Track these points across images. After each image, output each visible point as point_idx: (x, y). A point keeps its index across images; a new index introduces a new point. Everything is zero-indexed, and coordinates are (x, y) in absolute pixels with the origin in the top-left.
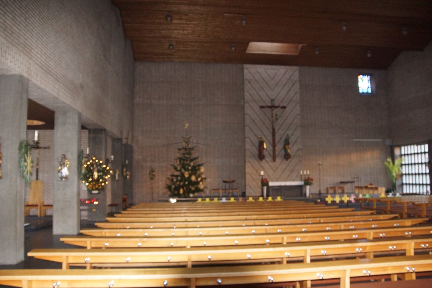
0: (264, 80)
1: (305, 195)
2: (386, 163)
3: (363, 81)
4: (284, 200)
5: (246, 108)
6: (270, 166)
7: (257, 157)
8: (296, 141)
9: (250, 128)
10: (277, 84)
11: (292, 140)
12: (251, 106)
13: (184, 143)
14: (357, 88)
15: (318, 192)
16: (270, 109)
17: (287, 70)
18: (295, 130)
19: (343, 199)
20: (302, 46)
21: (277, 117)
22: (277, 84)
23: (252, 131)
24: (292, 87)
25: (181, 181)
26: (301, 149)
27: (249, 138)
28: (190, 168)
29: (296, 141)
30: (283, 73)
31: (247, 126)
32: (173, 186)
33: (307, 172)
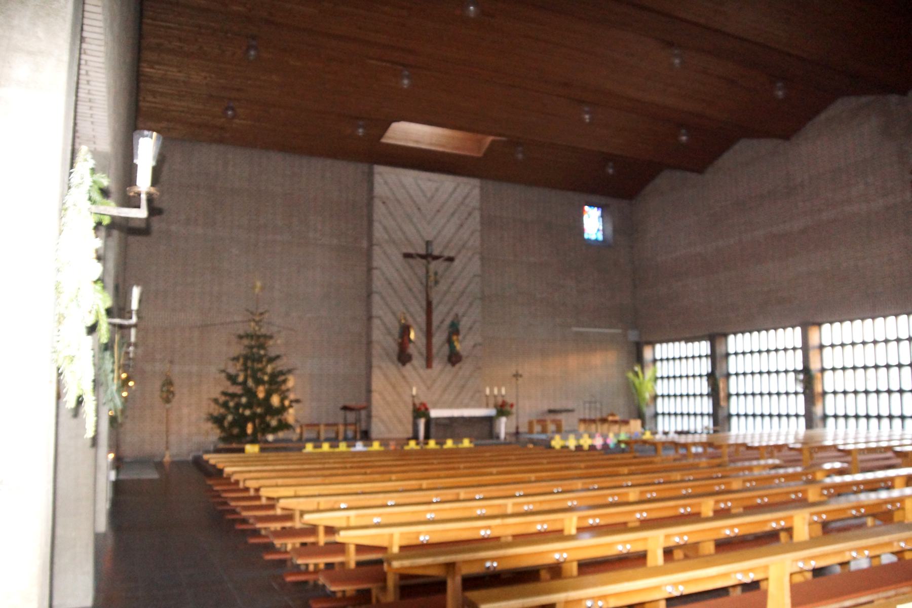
0: (414, 202)
1: (498, 437)
2: (630, 375)
3: (589, 217)
4: (476, 445)
6: (421, 377)
7: (395, 358)
9: (383, 298)
10: (438, 211)
11: (464, 324)
12: (385, 253)
13: (253, 324)
14: (582, 231)
16: (424, 261)
17: (458, 185)
18: (471, 304)
19: (582, 442)
20: (493, 142)
22: (438, 211)
24: (466, 219)
25: (246, 406)
27: (379, 317)
28: (266, 378)
29: (471, 328)
30: (450, 189)
32: (230, 418)
33: (499, 390)
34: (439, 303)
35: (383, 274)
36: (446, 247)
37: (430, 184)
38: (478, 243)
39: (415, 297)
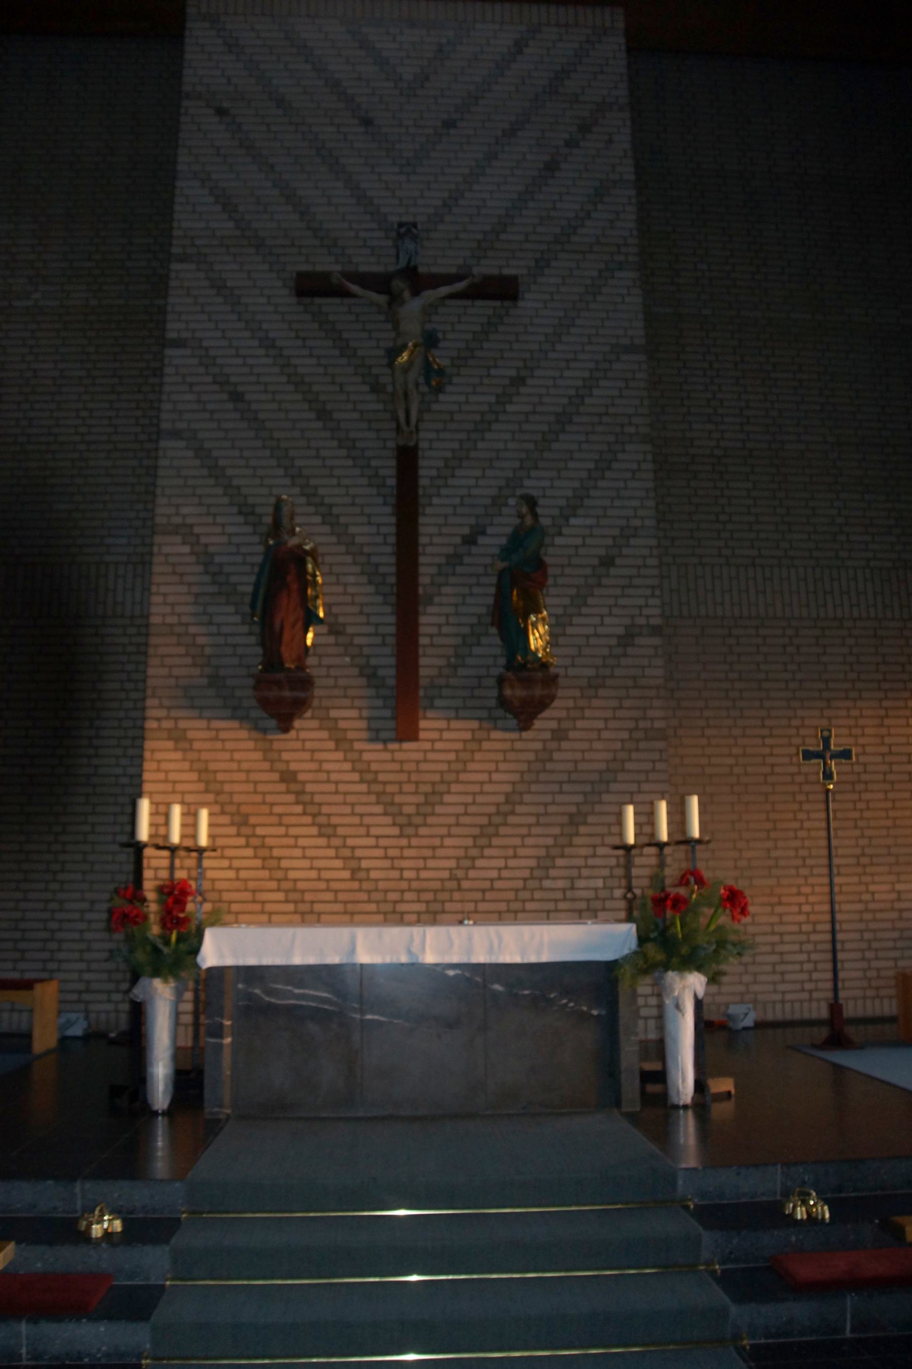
6: (368, 775)
8: (607, 562)
10: (449, 124)
21: (440, 358)
22: (449, 124)
24: (571, 144)
26: (656, 631)
29: (607, 562)
31: (176, 434)
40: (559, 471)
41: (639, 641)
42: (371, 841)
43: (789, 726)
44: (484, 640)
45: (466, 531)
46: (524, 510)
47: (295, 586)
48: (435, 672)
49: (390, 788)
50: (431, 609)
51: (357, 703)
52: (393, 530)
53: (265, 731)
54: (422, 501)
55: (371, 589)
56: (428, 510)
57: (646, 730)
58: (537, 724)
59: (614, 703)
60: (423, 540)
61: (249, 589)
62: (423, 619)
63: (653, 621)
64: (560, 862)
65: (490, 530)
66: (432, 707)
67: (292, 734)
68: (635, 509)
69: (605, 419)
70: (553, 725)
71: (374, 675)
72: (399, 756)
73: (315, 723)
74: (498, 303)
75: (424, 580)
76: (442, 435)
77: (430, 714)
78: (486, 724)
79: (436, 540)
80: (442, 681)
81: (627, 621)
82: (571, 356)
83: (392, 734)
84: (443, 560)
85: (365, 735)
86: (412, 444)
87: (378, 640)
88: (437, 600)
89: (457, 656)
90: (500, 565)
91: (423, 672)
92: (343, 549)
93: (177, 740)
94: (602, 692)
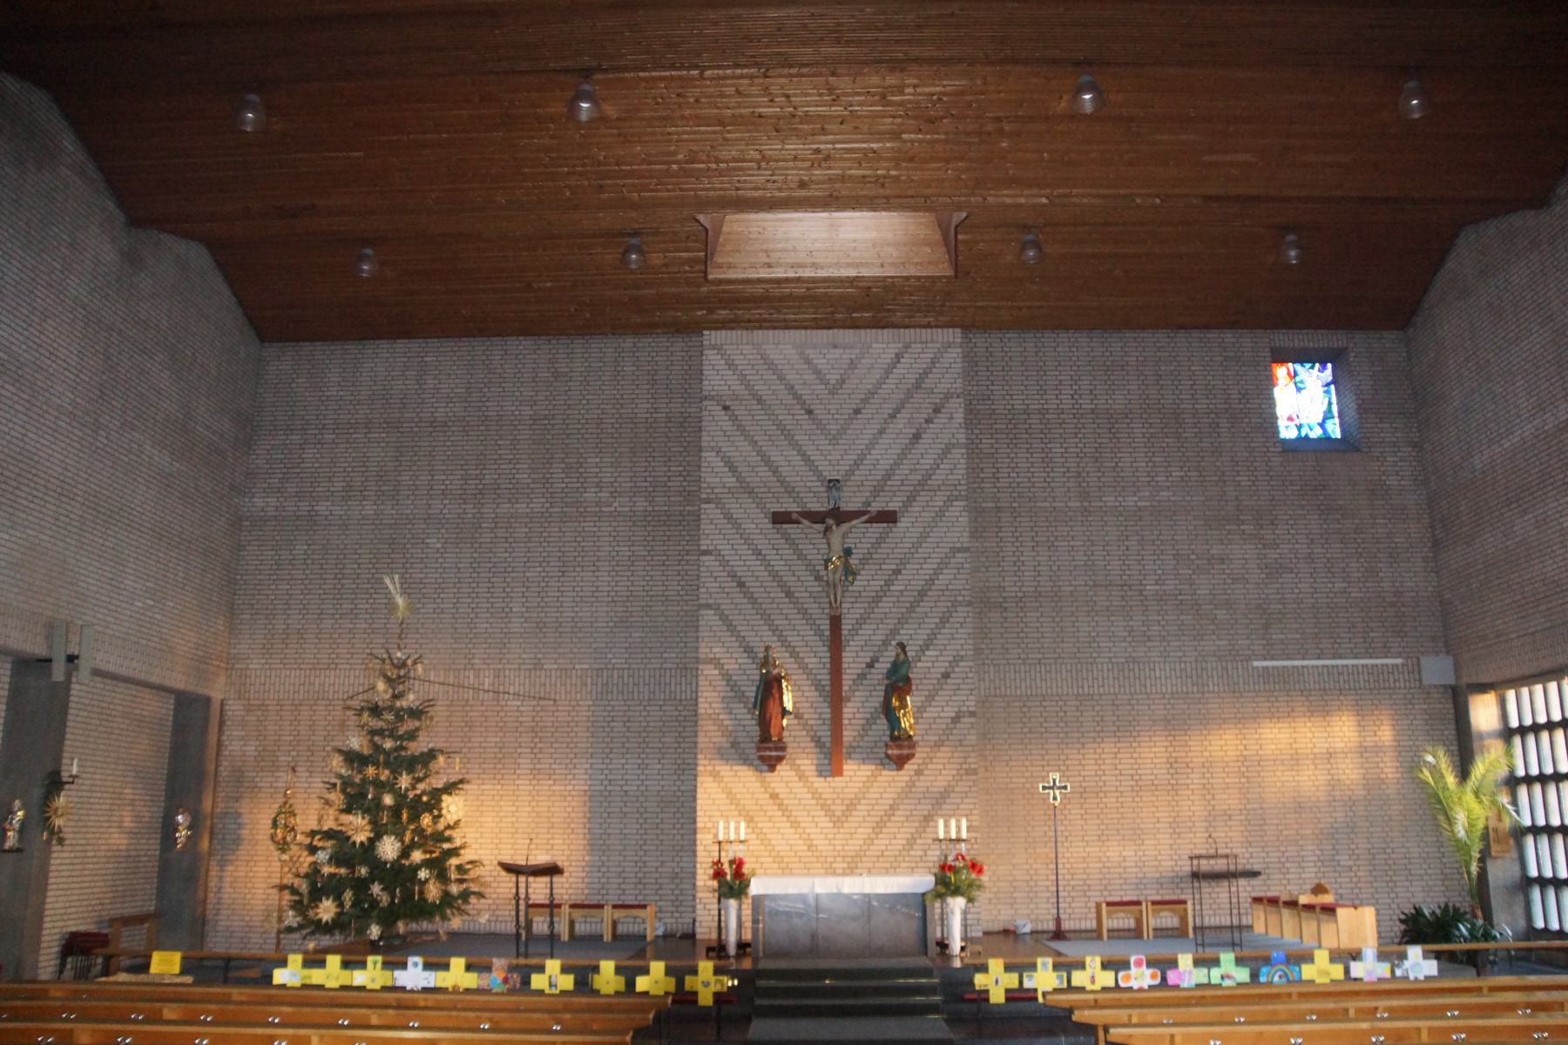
0: (797, 397)
3: (1299, 390)
5: (706, 526)
6: (816, 795)
7: (753, 753)
8: (946, 676)
9: (724, 618)
11: (924, 670)
12: (729, 517)
14: (1268, 421)
15: (1051, 926)
16: (820, 527)
17: (907, 346)
18: (944, 620)
21: (853, 561)
22: (857, 411)
23: (732, 629)
24: (929, 421)
26: (973, 714)
27: (716, 662)
29: (946, 676)
30: (888, 357)
31: (708, 606)
34: (862, 621)
35: (724, 563)
36: (877, 491)
37: (834, 354)
38: (960, 472)
39: (804, 612)
40: (920, 624)
41: (963, 720)
42: (818, 830)
43: (1059, 759)
44: (878, 721)
45: (868, 660)
46: (899, 651)
47: (777, 696)
48: (852, 739)
49: (828, 802)
50: (849, 704)
51: (810, 756)
52: (828, 660)
53: (761, 771)
54: (843, 643)
55: (817, 694)
56: (847, 649)
57: (966, 770)
58: (906, 766)
59: (949, 755)
60: (845, 666)
61: (753, 694)
62: (845, 710)
63: (971, 709)
64: (919, 841)
65: (881, 660)
66: (851, 758)
67: (776, 773)
68: (962, 645)
69: (946, 593)
70: (916, 767)
71: (819, 741)
72: (832, 784)
73: (788, 767)
74: (885, 525)
75: (845, 688)
76: (855, 605)
77: (849, 762)
78: (879, 767)
79: (851, 665)
80: (856, 744)
81: (957, 709)
82: (927, 555)
83: (828, 773)
84: (855, 677)
85: (815, 773)
86: (838, 614)
87: (821, 722)
88: (852, 699)
89: (863, 730)
90: (886, 682)
91: (845, 739)
92: (801, 671)
93: (715, 777)
94: (942, 749)
